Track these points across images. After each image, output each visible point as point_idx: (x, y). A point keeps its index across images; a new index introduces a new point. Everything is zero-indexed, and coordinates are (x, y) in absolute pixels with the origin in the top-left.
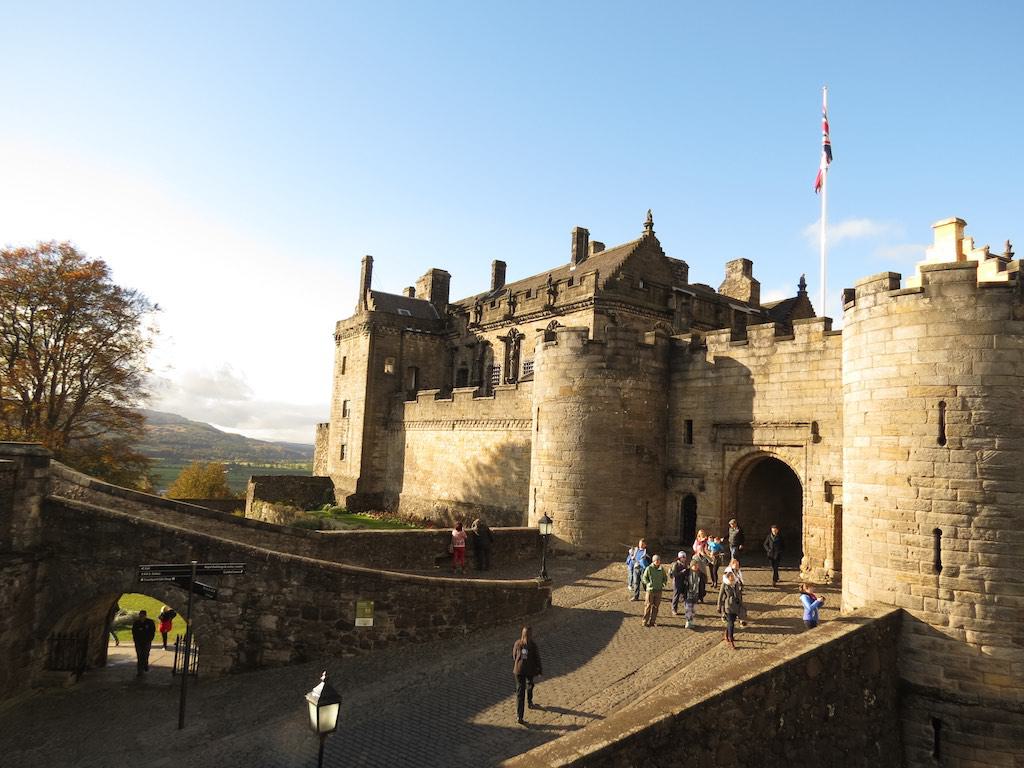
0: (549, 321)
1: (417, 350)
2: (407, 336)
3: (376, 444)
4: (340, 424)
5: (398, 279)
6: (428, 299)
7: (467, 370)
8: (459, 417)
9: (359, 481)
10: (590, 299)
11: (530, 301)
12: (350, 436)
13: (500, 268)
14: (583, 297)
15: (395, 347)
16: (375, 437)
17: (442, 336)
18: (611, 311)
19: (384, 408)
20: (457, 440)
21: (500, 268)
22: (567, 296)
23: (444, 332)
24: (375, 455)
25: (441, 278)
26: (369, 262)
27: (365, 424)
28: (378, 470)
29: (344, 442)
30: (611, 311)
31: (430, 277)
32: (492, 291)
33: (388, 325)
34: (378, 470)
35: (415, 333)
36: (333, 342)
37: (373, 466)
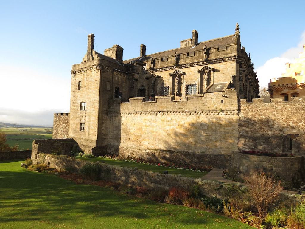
1: (118, 79)
2: (115, 73)
3: (103, 123)
5: (105, 47)
6: (114, 58)
7: (145, 90)
8: (160, 109)
9: (97, 141)
10: (235, 56)
13: (144, 48)
14: (229, 55)
15: (110, 77)
16: (103, 120)
17: (127, 74)
18: (242, 63)
19: (106, 106)
20: (159, 120)
21: (144, 48)
22: (216, 55)
23: (129, 72)
24: (103, 128)
25: (120, 50)
26: (93, 36)
27: (99, 113)
28: (104, 135)
29: (83, 121)
31: (115, 49)
32: (140, 58)
33: (108, 67)
34: (104, 135)
36: (70, 75)
37: (102, 133)
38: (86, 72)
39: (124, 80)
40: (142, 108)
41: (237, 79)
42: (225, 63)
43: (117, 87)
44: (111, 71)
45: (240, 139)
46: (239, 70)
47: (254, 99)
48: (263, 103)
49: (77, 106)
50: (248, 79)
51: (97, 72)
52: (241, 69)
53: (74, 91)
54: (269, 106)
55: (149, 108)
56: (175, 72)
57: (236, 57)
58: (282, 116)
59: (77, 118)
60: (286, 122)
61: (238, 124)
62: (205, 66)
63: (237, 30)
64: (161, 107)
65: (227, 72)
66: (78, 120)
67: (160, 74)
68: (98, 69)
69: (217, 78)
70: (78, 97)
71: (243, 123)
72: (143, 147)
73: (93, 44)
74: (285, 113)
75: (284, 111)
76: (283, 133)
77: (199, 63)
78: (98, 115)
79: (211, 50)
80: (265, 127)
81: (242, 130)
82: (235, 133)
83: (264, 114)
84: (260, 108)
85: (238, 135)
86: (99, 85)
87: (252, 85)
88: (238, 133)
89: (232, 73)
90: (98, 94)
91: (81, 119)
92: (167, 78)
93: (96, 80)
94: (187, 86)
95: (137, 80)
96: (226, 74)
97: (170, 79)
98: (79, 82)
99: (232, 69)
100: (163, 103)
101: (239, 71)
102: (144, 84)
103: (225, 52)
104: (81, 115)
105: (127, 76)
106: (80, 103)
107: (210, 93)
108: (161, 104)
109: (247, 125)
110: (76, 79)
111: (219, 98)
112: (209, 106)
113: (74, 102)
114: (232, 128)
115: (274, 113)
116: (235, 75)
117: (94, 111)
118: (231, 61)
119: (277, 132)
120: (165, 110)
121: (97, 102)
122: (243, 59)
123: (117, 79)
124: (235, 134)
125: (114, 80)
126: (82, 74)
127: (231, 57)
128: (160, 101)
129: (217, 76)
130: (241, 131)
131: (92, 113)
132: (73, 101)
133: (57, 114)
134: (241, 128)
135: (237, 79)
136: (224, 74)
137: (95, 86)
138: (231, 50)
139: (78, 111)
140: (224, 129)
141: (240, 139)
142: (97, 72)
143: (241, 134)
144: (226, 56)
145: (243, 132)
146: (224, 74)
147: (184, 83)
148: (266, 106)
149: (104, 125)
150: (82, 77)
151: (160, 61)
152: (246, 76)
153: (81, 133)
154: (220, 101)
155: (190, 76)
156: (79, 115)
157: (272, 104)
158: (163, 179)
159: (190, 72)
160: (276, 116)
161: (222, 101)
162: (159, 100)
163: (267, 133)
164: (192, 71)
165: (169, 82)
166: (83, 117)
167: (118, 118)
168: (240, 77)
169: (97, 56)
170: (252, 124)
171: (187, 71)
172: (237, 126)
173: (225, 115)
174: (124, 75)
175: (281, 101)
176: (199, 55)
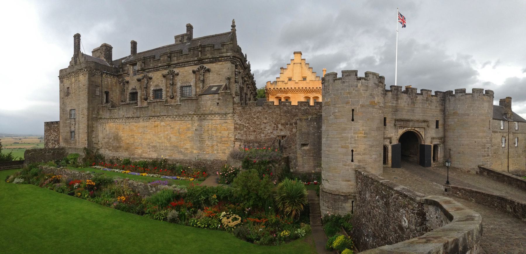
0: (198, 66)
41: (232, 80)
45: (236, 143)
50: (245, 81)
60: (275, 124)
61: (233, 127)
71: (238, 126)
74: (275, 116)
83: (258, 117)
85: (233, 139)
87: (249, 88)
94: (182, 87)
112: (204, 109)
115: (266, 116)
135: (232, 80)
140: (220, 133)
141: (236, 143)
143: (236, 137)
147: (179, 85)
152: (242, 78)
155: (185, 77)
158: (156, 190)
161: (218, 103)
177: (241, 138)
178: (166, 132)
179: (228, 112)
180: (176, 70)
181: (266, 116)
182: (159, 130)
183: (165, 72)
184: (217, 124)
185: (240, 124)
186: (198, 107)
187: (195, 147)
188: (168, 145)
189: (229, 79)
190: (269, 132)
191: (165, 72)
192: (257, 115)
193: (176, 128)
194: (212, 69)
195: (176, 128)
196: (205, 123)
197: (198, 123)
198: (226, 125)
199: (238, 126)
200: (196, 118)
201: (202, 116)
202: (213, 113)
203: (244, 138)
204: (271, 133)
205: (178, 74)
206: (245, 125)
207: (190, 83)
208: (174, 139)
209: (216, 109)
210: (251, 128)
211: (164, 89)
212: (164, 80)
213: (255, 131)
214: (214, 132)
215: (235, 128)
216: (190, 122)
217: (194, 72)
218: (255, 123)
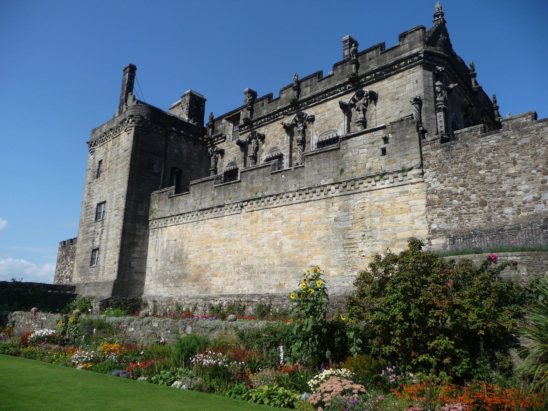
2: (172, 137)
4: (92, 228)
8: (249, 196)
10: (417, 55)
11: (323, 81)
12: (104, 237)
18: (439, 68)
22: (378, 62)
24: (135, 255)
26: (132, 69)
27: (125, 220)
28: (136, 272)
29: (97, 244)
30: (439, 68)
31: (187, 98)
34: (136, 272)
35: (179, 134)
38: (111, 138)
39: (195, 154)
40: (213, 199)
42: (400, 74)
43: (176, 168)
44: (161, 132)
46: (435, 86)
47: (459, 131)
48: (483, 136)
49: (90, 215)
51: (128, 132)
52: (438, 83)
53: (90, 183)
54: (499, 141)
55: (227, 196)
56: (295, 119)
57: (422, 55)
58: (535, 160)
59: (88, 238)
61: (424, 201)
62: (357, 91)
63: (438, 16)
64: (251, 190)
65: (405, 93)
66: (90, 243)
67: (266, 130)
68: (131, 125)
69: (383, 114)
70: (94, 194)
72: (213, 293)
73: (133, 84)
75: (537, 145)
76: (543, 205)
77: (343, 88)
78: (122, 224)
79: (367, 54)
80: (494, 197)
81: (436, 216)
82: (418, 227)
83: (489, 163)
84: (476, 151)
86: (129, 158)
88: (427, 225)
89: (417, 94)
90: (126, 179)
91: (93, 241)
92: (279, 136)
93: (125, 151)
95: (222, 152)
96: (402, 100)
97: (285, 137)
98: (100, 162)
99: (416, 85)
100: (254, 181)
101: (432, 89)
102: (235, 159)
103: (398, 50)
104: (94, 231)
105: (204, 148)
106: (95, 207)
107: (354, 139)
108: (252, 183)
109: (447, 200)
110: (94, 158)
111: (375, 144)
112: (353, 168)
113: (86, 207)
114: (410, 214)
115: (512, 155)
116: (422, 96)
117: (118, 217)
118: (412, 67)
119: (527, 205)
120: (259, 195)
121: (123, 197)
122: (441, 60)
123: (176, 150)
124: (418, 229)
125: (168, 152)
126: (105, 145)
127: (410, 57)
128: (249, 178)
129: (382, 107)
130: (432, 220)
131: (114, 223)
132: (87, 204)
133: (64, 242)
134: (433, 211)
136: (398, 99)
137: (124, 163)
138: (409, 43)
139: (91, 223)
140: (392, 220)
142: (128, 132)
143: (434, 226)
144: (399, 58)
145: (439, 220)
146: (398, 99)
147: (314, 139)
148: (490, 142)
149: (137, 249)
150: (104, 149)
151: (265, 102)
153: (92, 270)
154: (380, 152)
155: (326, 121)
156: (91, 232)
157: (505, 133)
159: (326, 113)
160: (519, 161)
162: (247, 175)
163: (500, 213)
164: (329, 110)
165: (283, 144)
166: (99, 235)
167: (167, 232)
168: (436, 102)
169: (135, 104)
170: (458, 196)
171: (319, 111)
172: (423, 208)
173: (391, 185)
174: (194, 144)
175: (529, 120)
176: (342, 71)
177: (445, 226)
178: (274, 233)
179: (409, 166)
180: (309, 112)
181: (512, 155)
182: (260, 230)
183: (289, 120)
184: (384, 200)
185: (442, 192)
186: (340, 167)
187: (332, 262)
188: (277, 261)
189: (418, 101)
190: (529, 197)
191: (289, 120)
192: (486, 159)
193: (293, 222)
194: (380, 94)
195: (293, 222)
196: (356, 201)
197: (341, 203)
198: (404, 198)
199: (436, 197)
200: (334, 191)
201: (349, 185)
202: (373, 173)
203: (455, 226)
204: (536, 200)
205: (312, 119)
206: (454, 190)
207: (336, 131)
208: (288, 248)
209: (379, 164)
210: (473, 196)
211: (286, 154)
212: (287, 138)
213: (483, 204)
214: (377, 220)
215: (430, 204)
216: (323, 203)
217: (343, 106)
218: (482, 180)
